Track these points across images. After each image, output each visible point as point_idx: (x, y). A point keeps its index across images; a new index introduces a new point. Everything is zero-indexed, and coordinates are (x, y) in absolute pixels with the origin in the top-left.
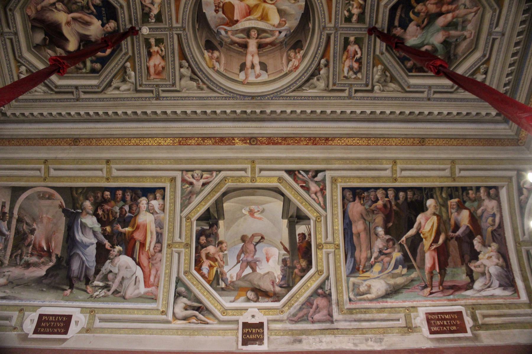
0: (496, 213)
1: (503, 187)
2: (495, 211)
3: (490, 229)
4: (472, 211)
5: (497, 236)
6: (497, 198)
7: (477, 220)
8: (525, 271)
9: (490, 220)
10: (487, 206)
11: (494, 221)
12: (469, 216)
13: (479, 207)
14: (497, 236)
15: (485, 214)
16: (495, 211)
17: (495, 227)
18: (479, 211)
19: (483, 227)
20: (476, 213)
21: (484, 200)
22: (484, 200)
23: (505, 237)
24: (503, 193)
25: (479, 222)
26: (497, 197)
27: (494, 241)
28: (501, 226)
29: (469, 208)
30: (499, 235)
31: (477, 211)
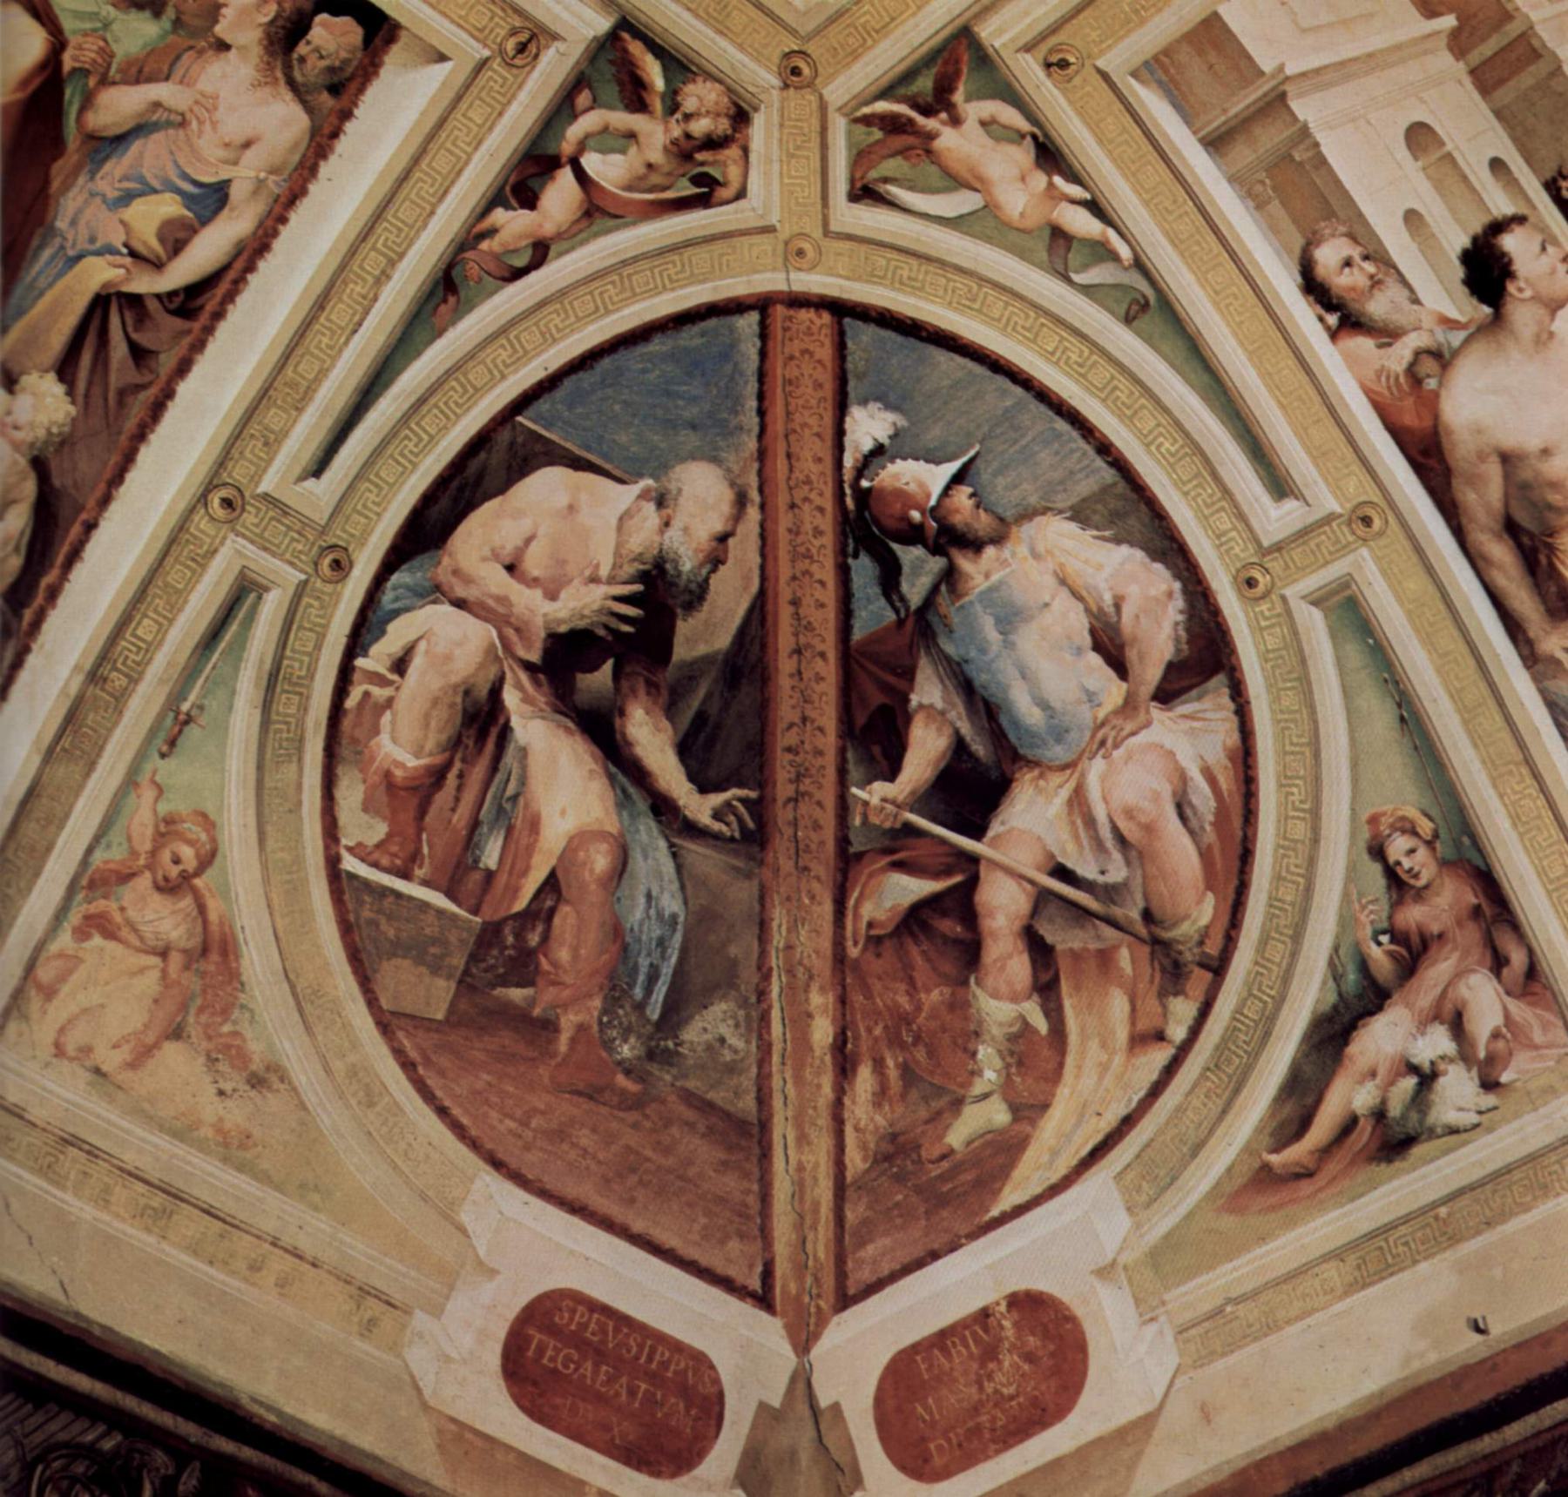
0: (237, 192)
1: (442, 58)
2: (244, 176)
3: (99, 273)
4: (68, 62)
5: (119, 350)
6: (326, 100)
7: (56, 145)
8: (120, 699)
9: (149, 217)
10: (209, 103)
11: (176, 239)
12: (24, 83)
13: (138, 73)
14: (119, 350)
15: (149, 155)
16: (244, 176)
17: (145, 284)
18: (118, 105)
19: (61, 224)
20: (88, 101)
21: (223, 46)
22: (223, 46)
23: (169, 394)
24: (399, 102)
25: (59, 170)
26: (335, 97)
27: (65, 369)
28: (199, 304)
29: (68, 24)
30: (140, 354)
31: (105, 81)
